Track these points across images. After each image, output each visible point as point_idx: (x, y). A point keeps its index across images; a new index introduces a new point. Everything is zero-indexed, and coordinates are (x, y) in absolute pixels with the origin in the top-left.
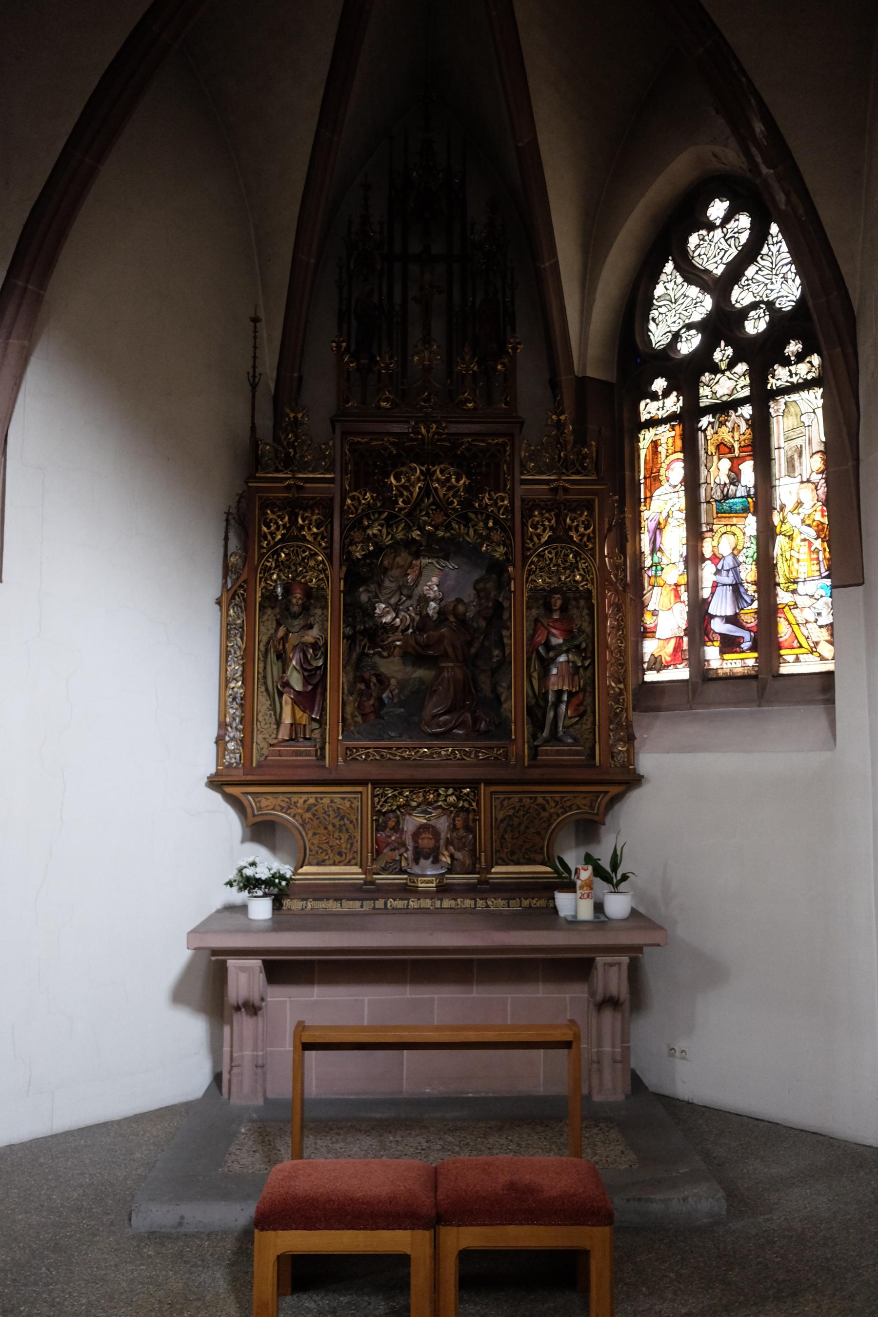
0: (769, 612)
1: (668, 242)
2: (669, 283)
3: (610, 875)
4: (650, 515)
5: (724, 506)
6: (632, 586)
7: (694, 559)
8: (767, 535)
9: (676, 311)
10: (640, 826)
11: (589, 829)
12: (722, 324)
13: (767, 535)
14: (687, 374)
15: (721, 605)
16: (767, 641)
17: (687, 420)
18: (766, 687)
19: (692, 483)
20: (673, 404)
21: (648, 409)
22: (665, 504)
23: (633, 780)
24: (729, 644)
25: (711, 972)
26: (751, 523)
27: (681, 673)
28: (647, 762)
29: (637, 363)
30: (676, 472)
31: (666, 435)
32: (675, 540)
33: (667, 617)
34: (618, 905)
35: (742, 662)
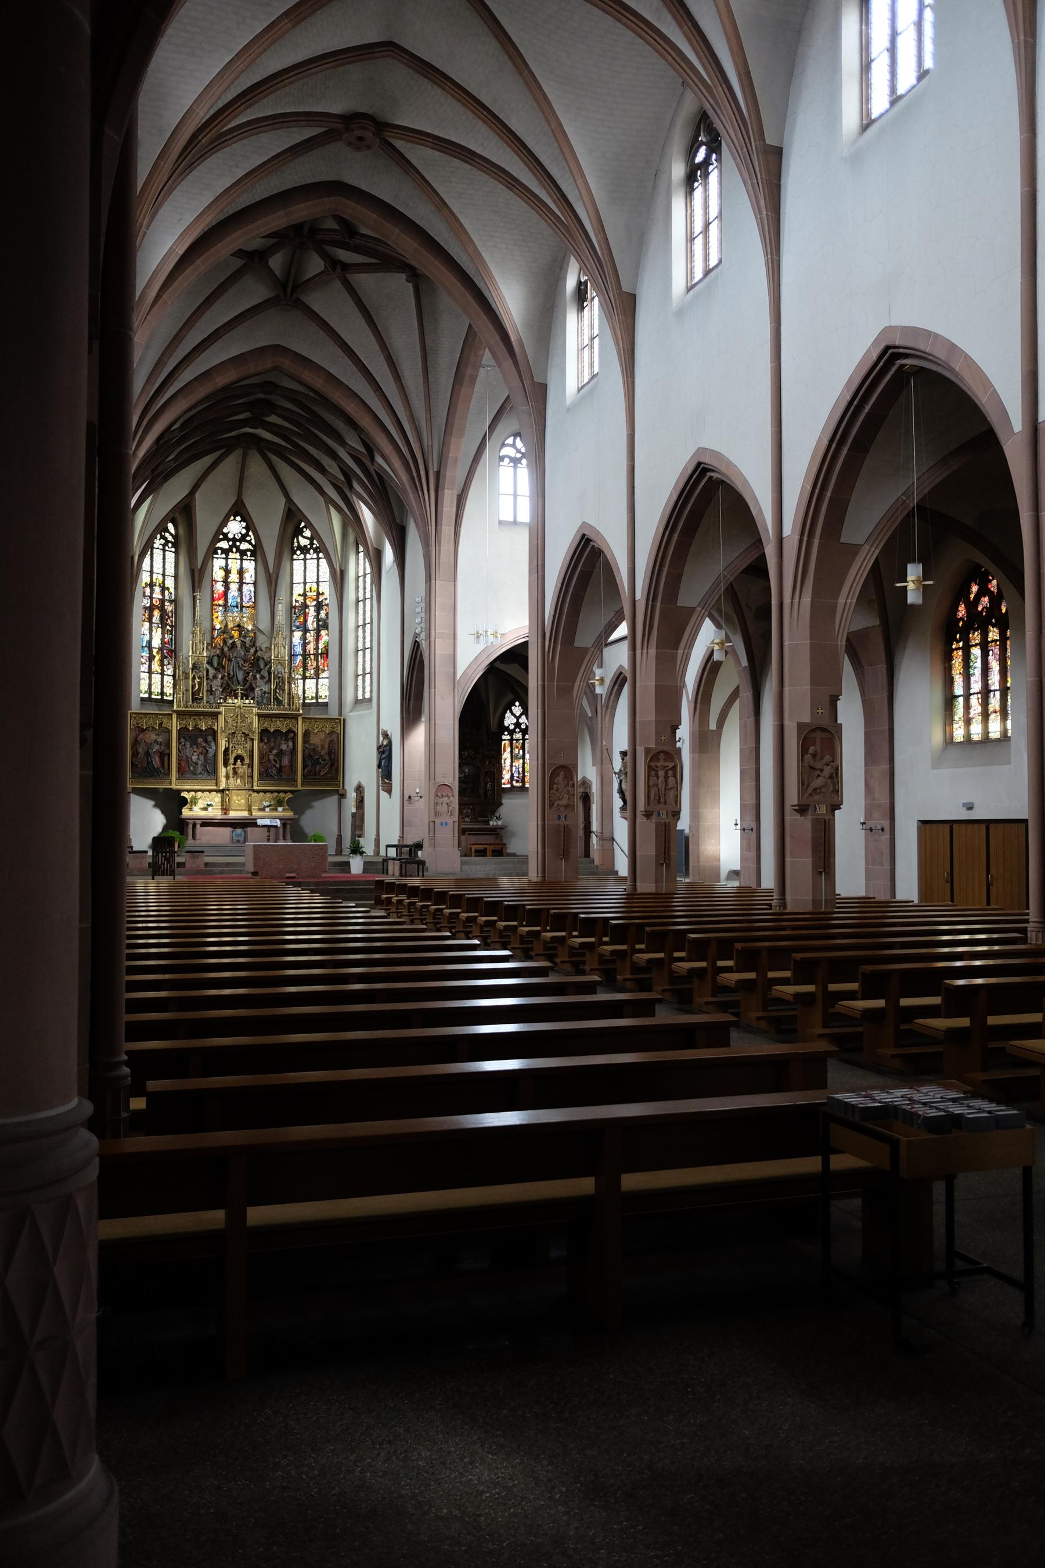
0: (524, 776)
1: (509, 707)
2: (508, 714)
3: (498, 818)
4: (503, 757)
5: (517, 757)
6: (500, 770)
7: (511, 766)
8: (524, 763)
9: (509, 721)
10: (503, 811)
11: (493, 812)
12: (518, 725)
13: (524, 763)
14: (512, 733)
15: (516, 775)
16: (523, 781)
17: (511, 740)
18: (523, 789)
19: (512, 752)
20: (509, 737)
21: (504, 737)
22: (506, 755)
23: (502, 804)
24: (517, 781)
25: (513, 834)
26: (521, 761)
27: (509, 786)
28: (504, 801)
29: (504, 729)
30: (508, 749)
31: (507, 742)
32: (508, 762)
33: (506, 776)
34: (500, 823)
35: (519, 784)
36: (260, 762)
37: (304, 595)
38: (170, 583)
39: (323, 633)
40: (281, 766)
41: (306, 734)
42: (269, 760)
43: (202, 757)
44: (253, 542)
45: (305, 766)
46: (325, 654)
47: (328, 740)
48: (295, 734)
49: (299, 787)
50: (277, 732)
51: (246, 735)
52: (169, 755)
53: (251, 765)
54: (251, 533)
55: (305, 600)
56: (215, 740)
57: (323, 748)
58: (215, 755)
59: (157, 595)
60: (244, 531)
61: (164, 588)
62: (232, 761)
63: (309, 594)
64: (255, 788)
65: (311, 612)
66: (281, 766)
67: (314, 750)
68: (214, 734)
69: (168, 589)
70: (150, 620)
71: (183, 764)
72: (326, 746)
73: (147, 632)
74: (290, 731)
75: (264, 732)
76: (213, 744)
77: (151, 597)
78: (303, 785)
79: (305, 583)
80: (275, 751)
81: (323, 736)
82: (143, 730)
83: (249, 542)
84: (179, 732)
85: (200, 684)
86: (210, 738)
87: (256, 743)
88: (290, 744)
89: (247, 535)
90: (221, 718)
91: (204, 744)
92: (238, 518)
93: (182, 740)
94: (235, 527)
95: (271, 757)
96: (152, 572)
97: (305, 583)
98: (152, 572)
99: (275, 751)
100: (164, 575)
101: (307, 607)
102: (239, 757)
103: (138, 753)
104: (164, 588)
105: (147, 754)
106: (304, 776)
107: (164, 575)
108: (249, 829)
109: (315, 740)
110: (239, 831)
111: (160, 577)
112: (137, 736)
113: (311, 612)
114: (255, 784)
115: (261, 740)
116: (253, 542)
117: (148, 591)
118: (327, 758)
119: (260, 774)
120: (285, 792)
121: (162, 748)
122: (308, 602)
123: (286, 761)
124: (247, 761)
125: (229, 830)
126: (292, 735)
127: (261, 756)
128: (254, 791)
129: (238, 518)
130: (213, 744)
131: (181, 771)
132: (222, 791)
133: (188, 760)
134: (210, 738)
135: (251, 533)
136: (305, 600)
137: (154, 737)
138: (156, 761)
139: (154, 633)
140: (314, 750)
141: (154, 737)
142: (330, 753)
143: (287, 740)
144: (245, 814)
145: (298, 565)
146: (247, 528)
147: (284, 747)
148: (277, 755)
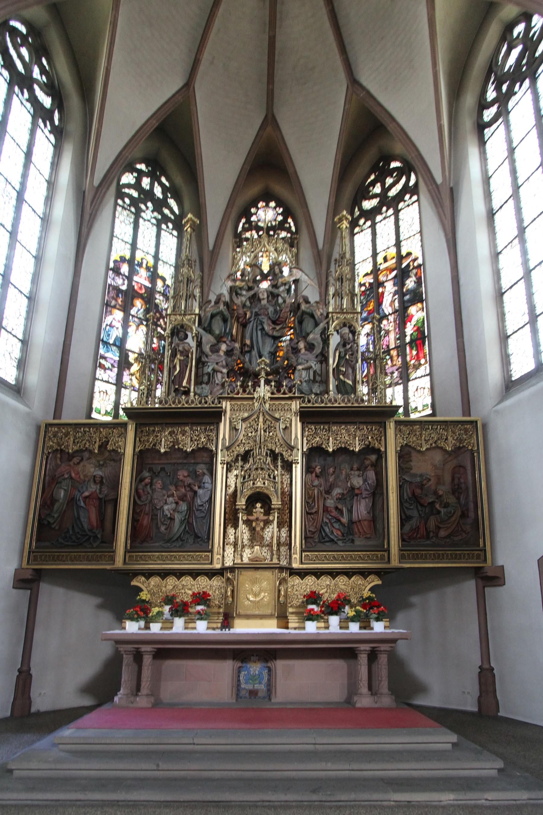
36: (307, 513)
37: (375, 271)
38: (166, 271)
39: (412, 310)
40: (351, 522)
41: (404, 455)
42: (326, 510)
43: (183, 507)
44: (293, 229)
45: (404, 520)
46: (420, 339)
47: (449, 466)
48: (381, 455)
49: (395, 562)
50: (343, 451)
51: (274, 456)
52: (115, 502)
53: (286, 522)
54: (290, 220)
55: (376, 278)
56: (212, 472)
57: (439, 480)
58: (211, 501)
59: (142, 279)
60: (280, 218)
61: (154, 276)
62: (241, 502)
63: (382, 267)
64: (296, 565)
65: (390, 288)
66: (351, 522)
67: (421, 486)
68: (210, 456)
69: (164, 280)
70: (126, 308)
71: (146, 521)
72: (448, 478)
73: (119, 325)
74: (368, 450)
75: (315, 453)
76: (207, 479)
77: (130, 278)
78: (402, 558)
79: (375, 255)
80: (337, 491)
81: (438, 457)
82: (71, 457)
83: (289, 230)
84: (143, 457)
85: (184, 365)
86: (201, 468)
87: (298, 471)
88: (371, 474)
89: (285, 221)
90: (224, 429)
91: (189, 480)
92: (272, 204)
93: (146, 474)
94: (266, 214)
95: (330, 503)
96: (134, 246)
97: (375, 255)
98: (134, 246)
99: (337, 491)
100: (156, 257)
101: (381, 284)
102: (259, 498)
103: (53, 501)
104: (154, 276)
105: (72, 501)
106: (404, 539)
107: (156, 257)
108: (280, 665)
109: (422, 467)
110: (255, 668)
111: (151, 262)
112: (58, 466)
113: (389, 289)
114: (296, 556)
115: (308, 469)
116: (293, 229)
117: (125, 269)
118: (452, 500)
119: (307, 537)
120: (364, 573)
121: (105, 490)
122: (382, 278)
123: (361, 509)
124: (276, 502)
125: (227, 667)
126: (373, 457)
127: (309, 500)
128: (293, 572)
129: (272, 204)
130: (207, 479)
131: (138, 537)
132: (221, 572)
133: (155, 511)
134: (201, 468)
135: (290, 220)
136: (376, 278)
137: (91, 469)
138: (89, 517)
139: (129, 330)
140: (421, 486)
141: (91, 469)
142: (457, 489)
143: (362, 468)
144: (269, 627)
145: (362, 241)
146: (287, 214)
147: (357, 482)
148: (341, 498)
